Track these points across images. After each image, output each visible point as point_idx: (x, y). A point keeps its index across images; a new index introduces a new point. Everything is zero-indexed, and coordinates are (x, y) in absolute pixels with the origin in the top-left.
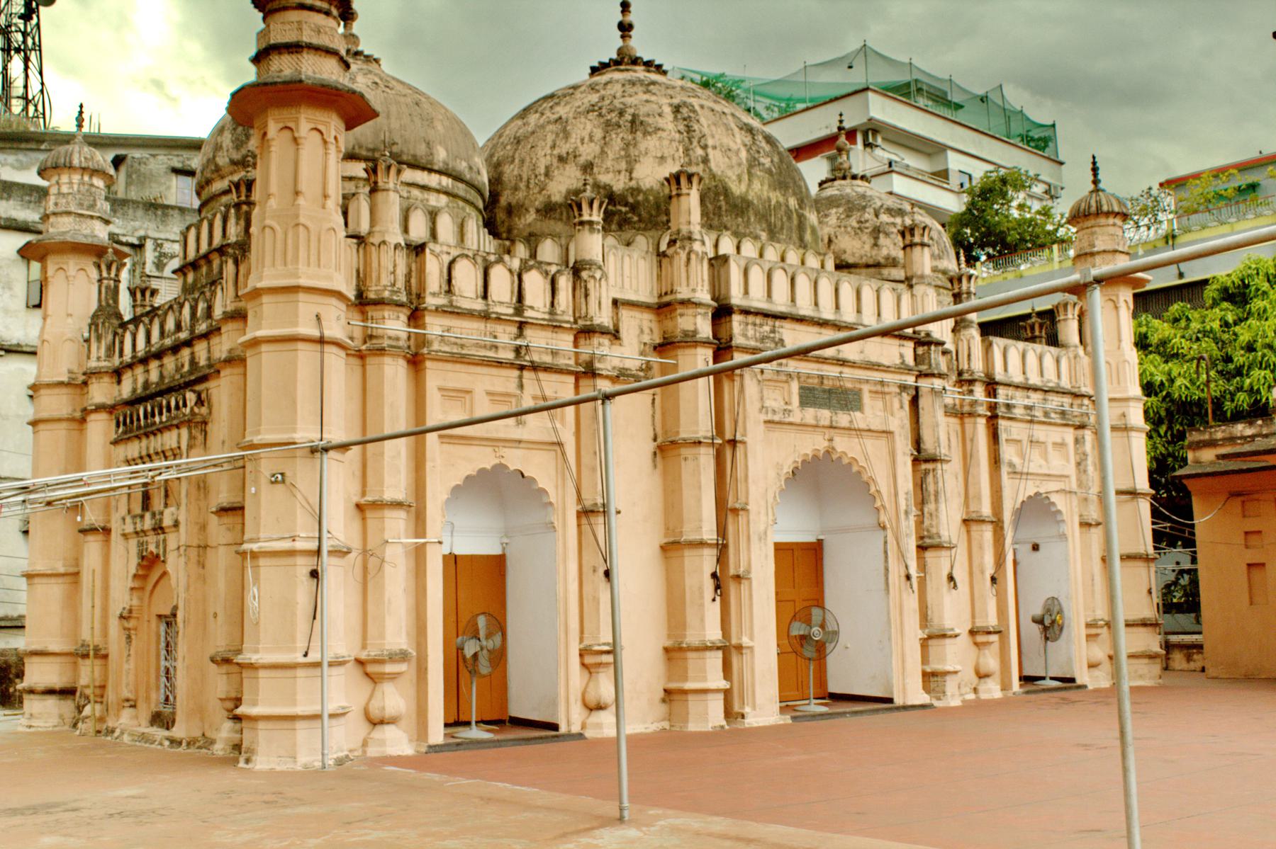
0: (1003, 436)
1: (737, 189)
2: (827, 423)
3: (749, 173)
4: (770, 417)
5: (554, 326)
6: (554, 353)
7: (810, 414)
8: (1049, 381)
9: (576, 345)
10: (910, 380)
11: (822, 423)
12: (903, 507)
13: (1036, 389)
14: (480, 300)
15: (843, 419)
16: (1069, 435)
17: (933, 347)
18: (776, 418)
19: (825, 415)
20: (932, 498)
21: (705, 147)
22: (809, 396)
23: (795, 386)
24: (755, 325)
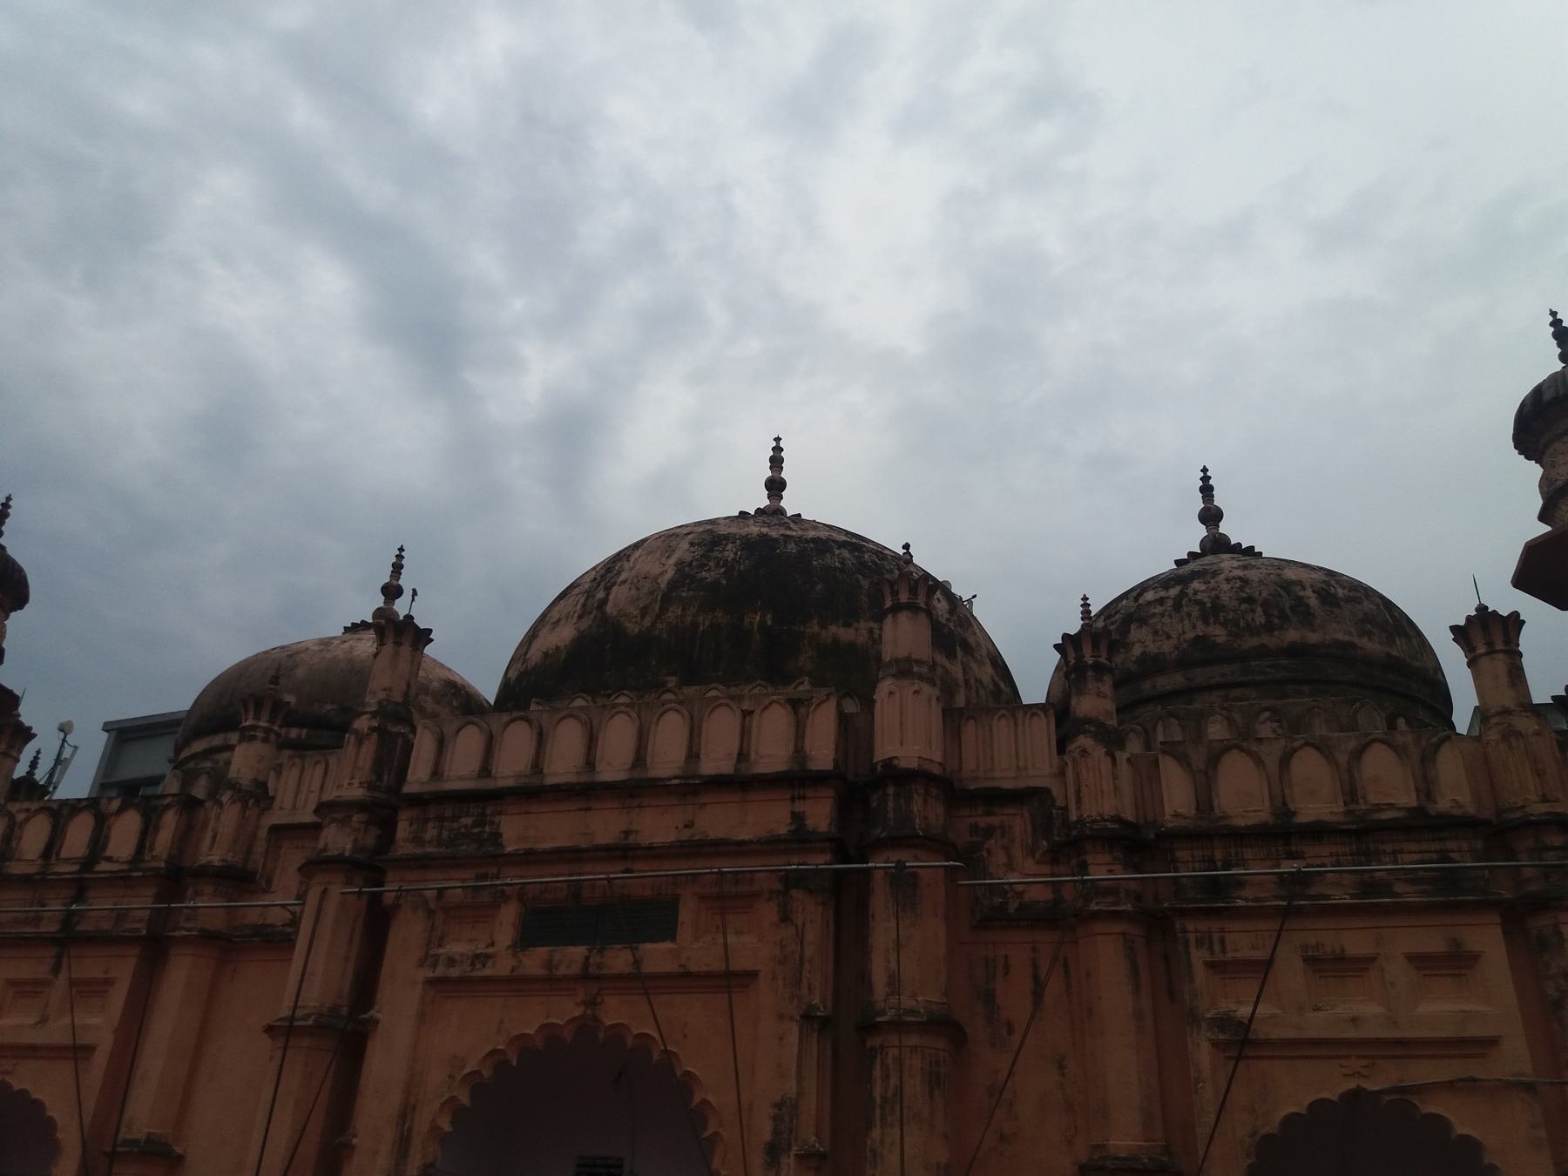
0: (1198, 957)
1: (632, 628)
2: (575, 970)
3: (667, 600)
4: (440, 971)
5: (123, 880)
6: (121, 915)
7: (534, 961)
8: (1379, 808)
9: (158, 898)
10: (820, 861)
11: (562, 971)
12: (764, 1130)
13: (1318, 832)
14: (39, 862)
15: (618, 960)
16: (1487, 939)
17: (891, 790)
18: (455, 972)
19: (573, 956)
20: (878, 1112)
21: (608, 589)
22: (541, 924)
23: (509, 914)
24: (441, 819)
